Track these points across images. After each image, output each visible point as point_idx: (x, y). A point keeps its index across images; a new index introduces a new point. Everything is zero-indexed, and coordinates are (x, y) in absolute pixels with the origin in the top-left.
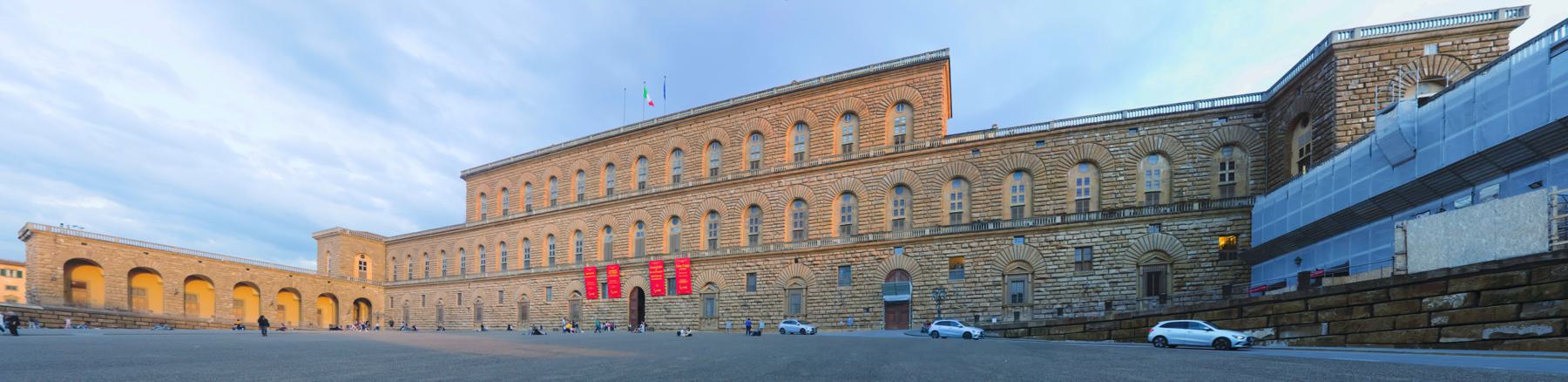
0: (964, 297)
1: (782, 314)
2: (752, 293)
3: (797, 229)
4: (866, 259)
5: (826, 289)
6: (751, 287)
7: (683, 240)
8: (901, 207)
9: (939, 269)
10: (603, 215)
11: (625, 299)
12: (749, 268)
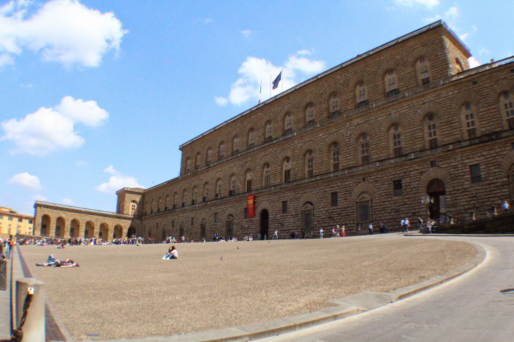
0: (482, 197)
1: (355, 222)
2: (335, 207)
3: (364, 155)
4: (412, 173)
5: (384, 200)
6: (334, 202)
7: (292, 173)
8: (434, 130)
9: (463, 176)
10: (247, 162)
11: (257, 218)
12: (332, 189)
